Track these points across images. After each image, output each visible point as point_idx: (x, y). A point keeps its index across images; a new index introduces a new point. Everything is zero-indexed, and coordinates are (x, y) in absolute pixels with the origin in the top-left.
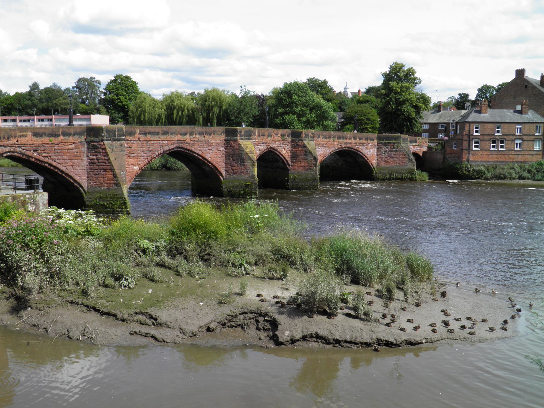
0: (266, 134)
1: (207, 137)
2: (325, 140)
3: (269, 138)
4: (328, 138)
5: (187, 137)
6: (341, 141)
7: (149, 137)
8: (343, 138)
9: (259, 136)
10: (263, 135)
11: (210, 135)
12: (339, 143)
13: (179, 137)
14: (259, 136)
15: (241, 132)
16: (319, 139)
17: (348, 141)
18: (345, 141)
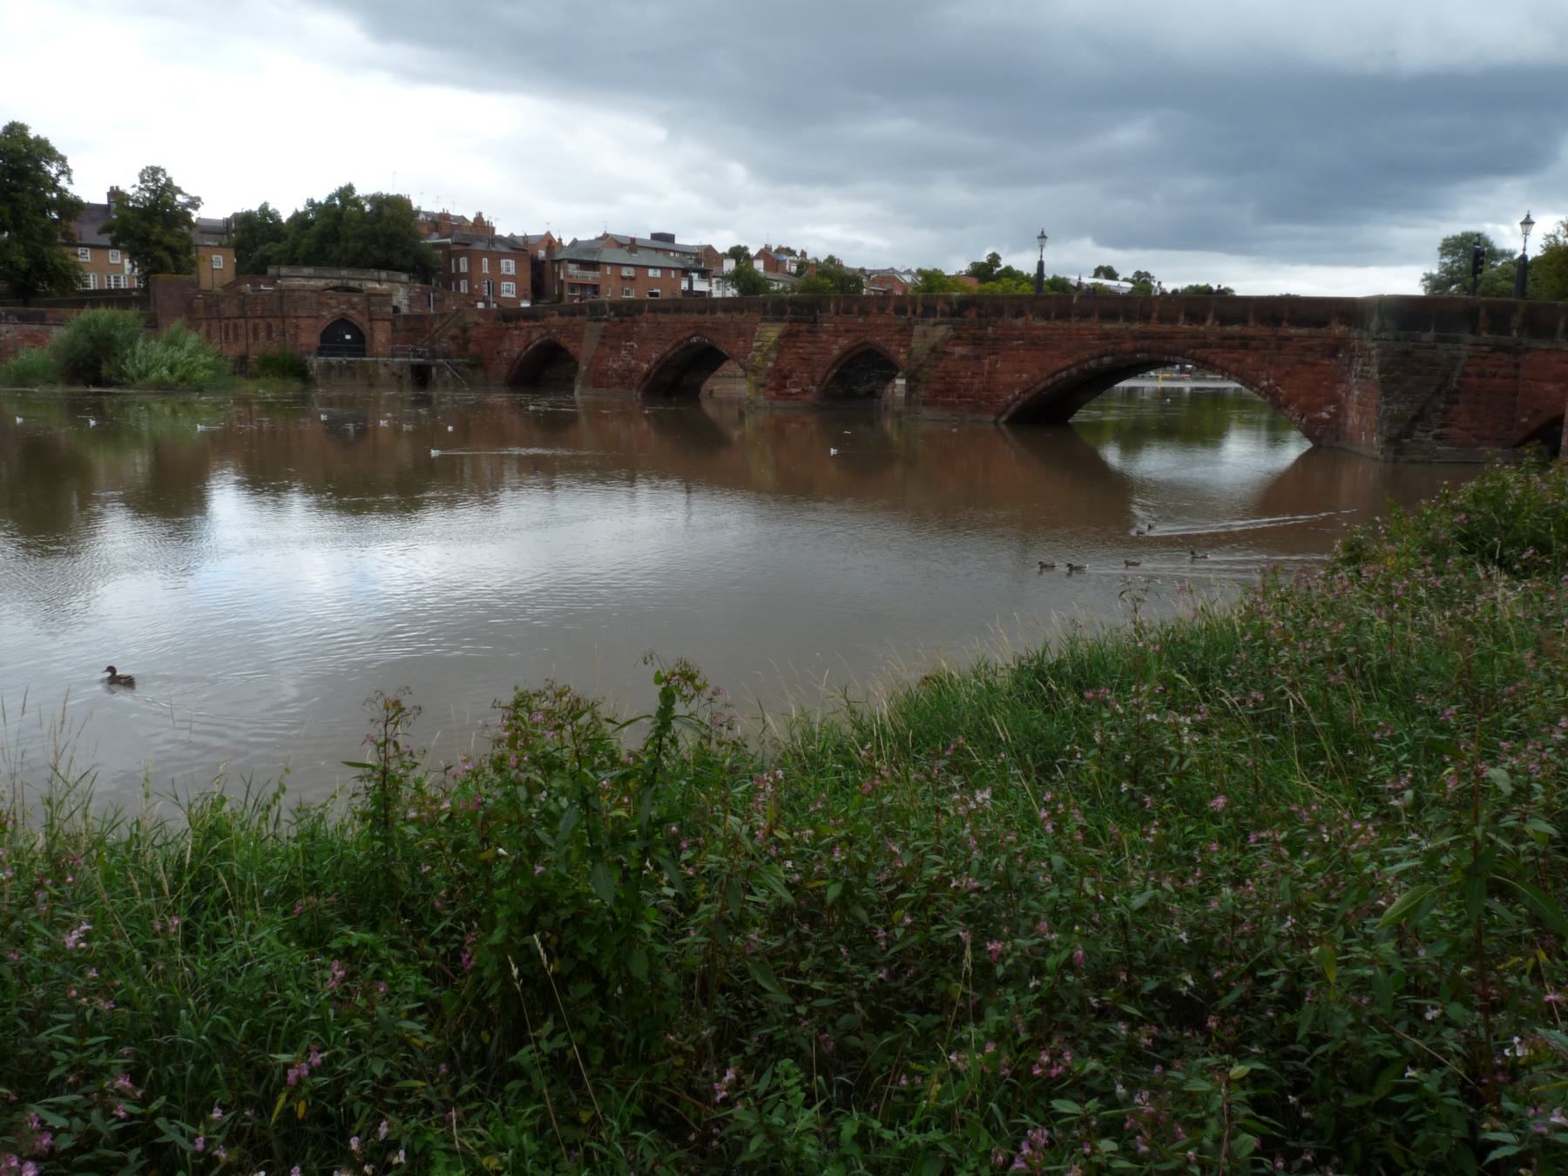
0: (855, 309)
1: (737, 317)
2: (1040, 323)
3: (860, 320)
4: (1059, 317)
5: (707, 316)
6: (1120, 325)
7: (661, 317)
8: (1129, 317)
9: (837, 313)
10: (847, 311)
11: (742, 312)
12: (1106, 336)
13: (696, 317)
14: (837, 313)
15: (765, 304)
16: (1020, 322)
17: (1154, 327)
18: (1137, 326)
